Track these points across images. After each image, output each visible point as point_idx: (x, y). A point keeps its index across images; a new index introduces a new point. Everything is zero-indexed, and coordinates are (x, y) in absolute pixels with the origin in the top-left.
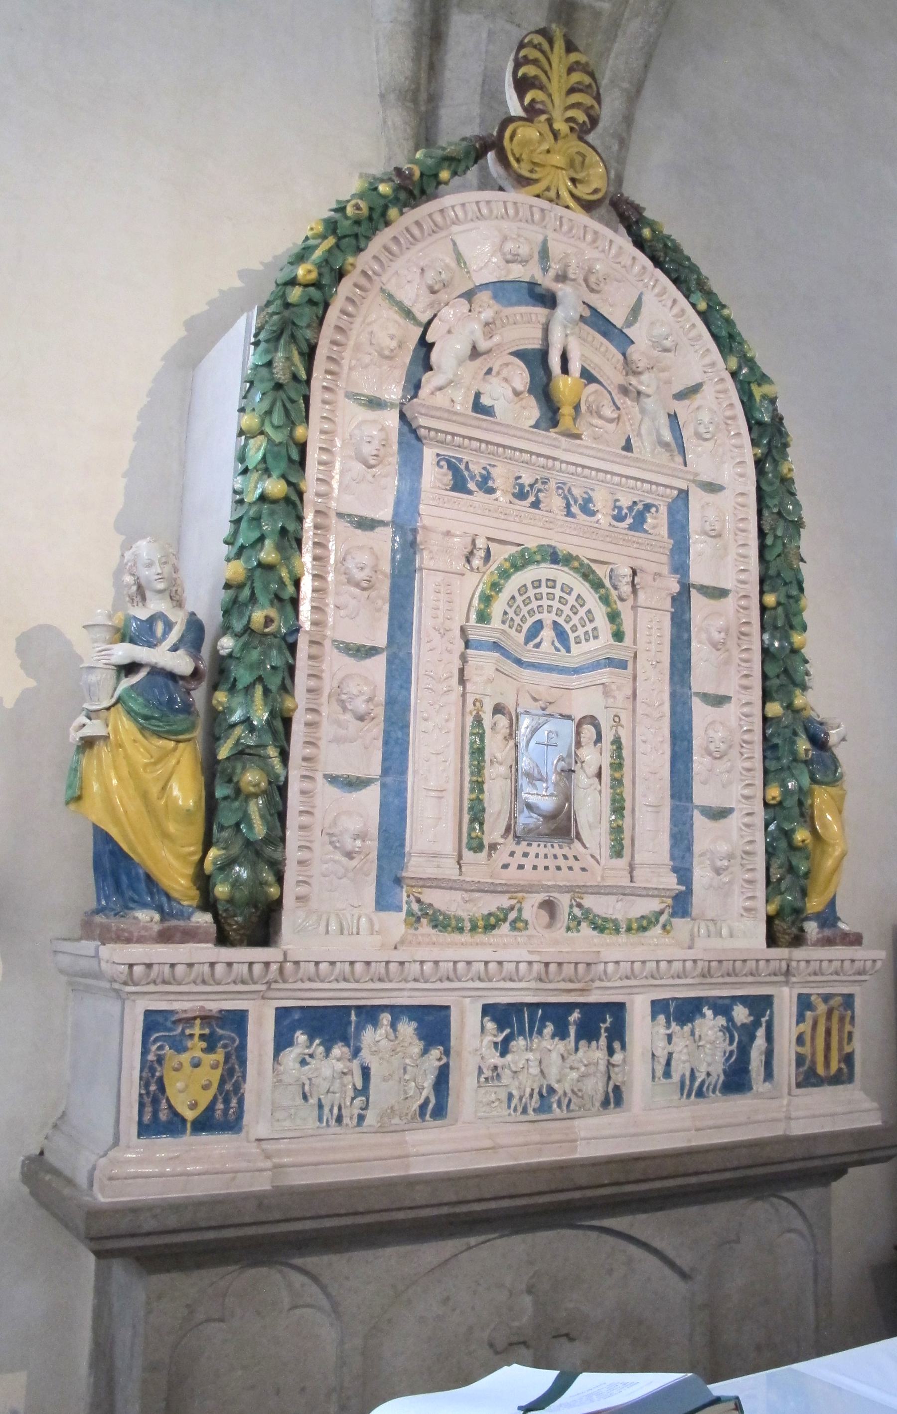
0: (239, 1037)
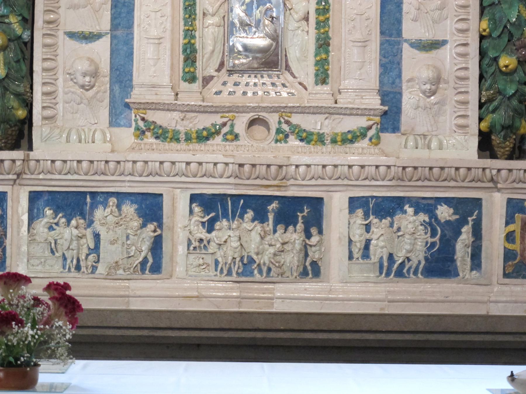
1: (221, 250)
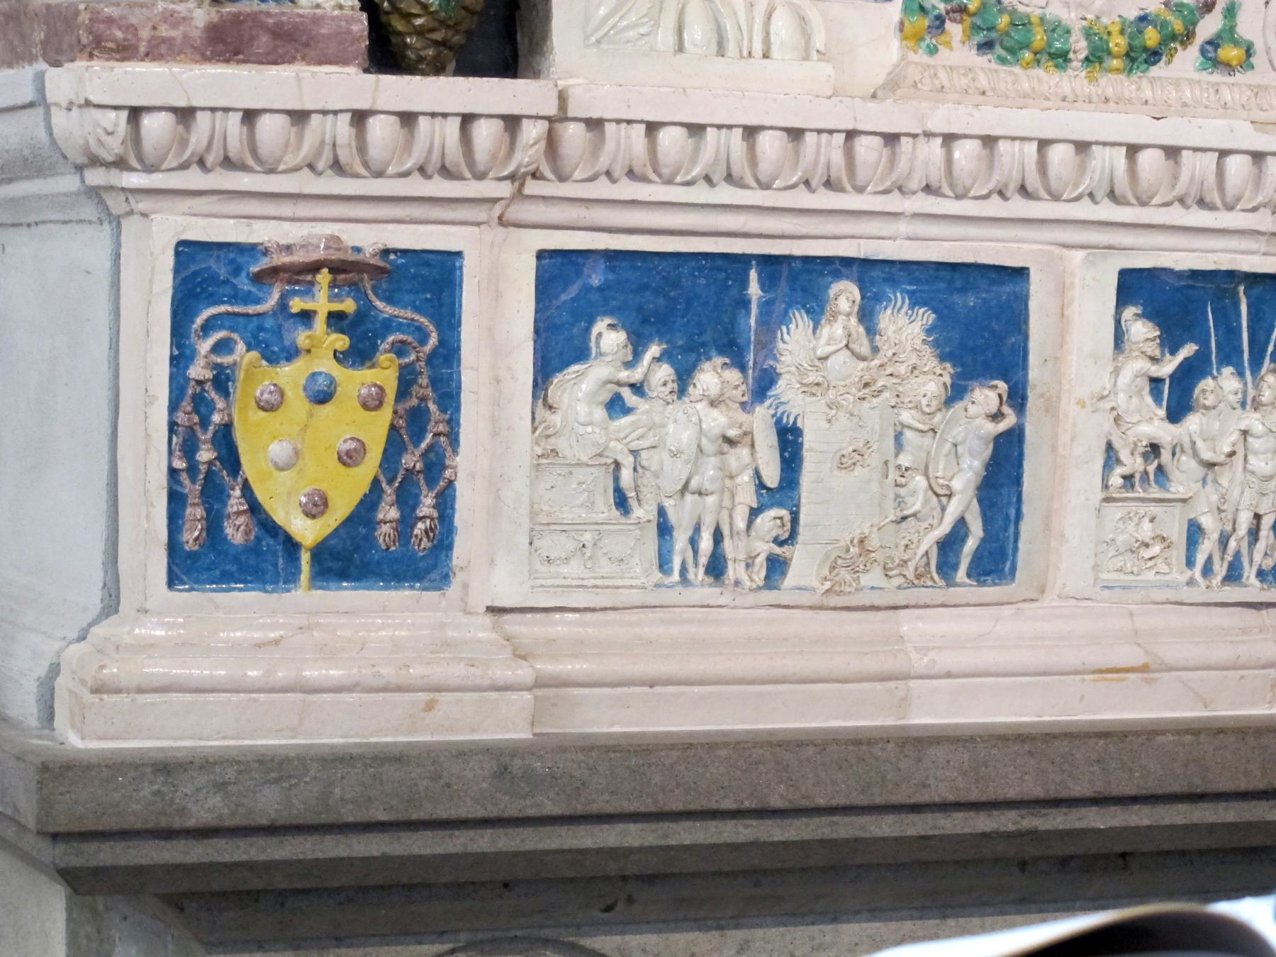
0: (438, 327)
1: (1210, 487)
